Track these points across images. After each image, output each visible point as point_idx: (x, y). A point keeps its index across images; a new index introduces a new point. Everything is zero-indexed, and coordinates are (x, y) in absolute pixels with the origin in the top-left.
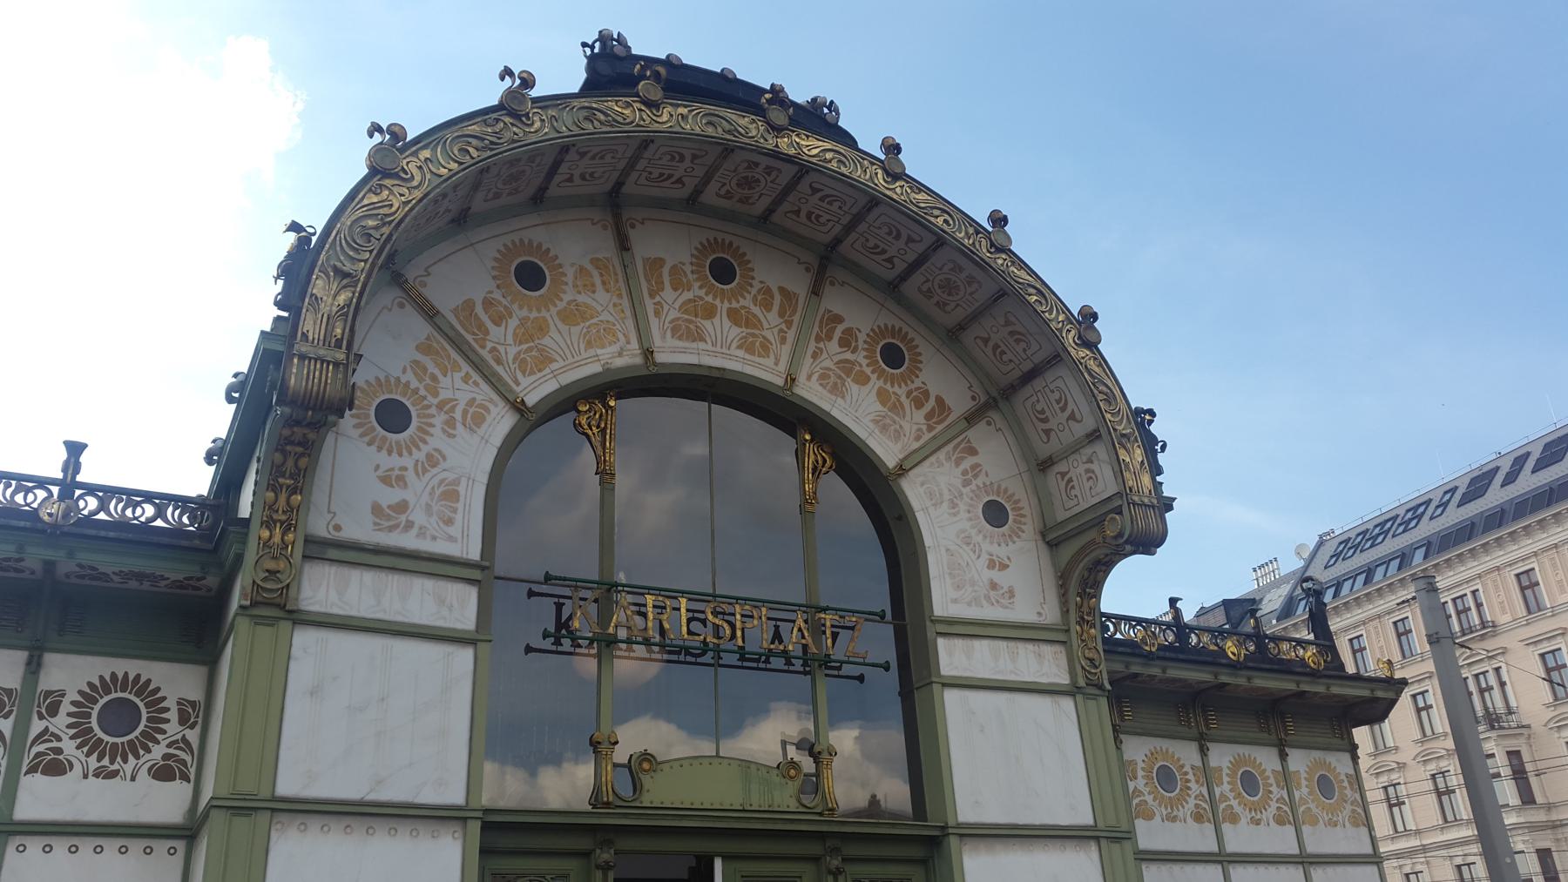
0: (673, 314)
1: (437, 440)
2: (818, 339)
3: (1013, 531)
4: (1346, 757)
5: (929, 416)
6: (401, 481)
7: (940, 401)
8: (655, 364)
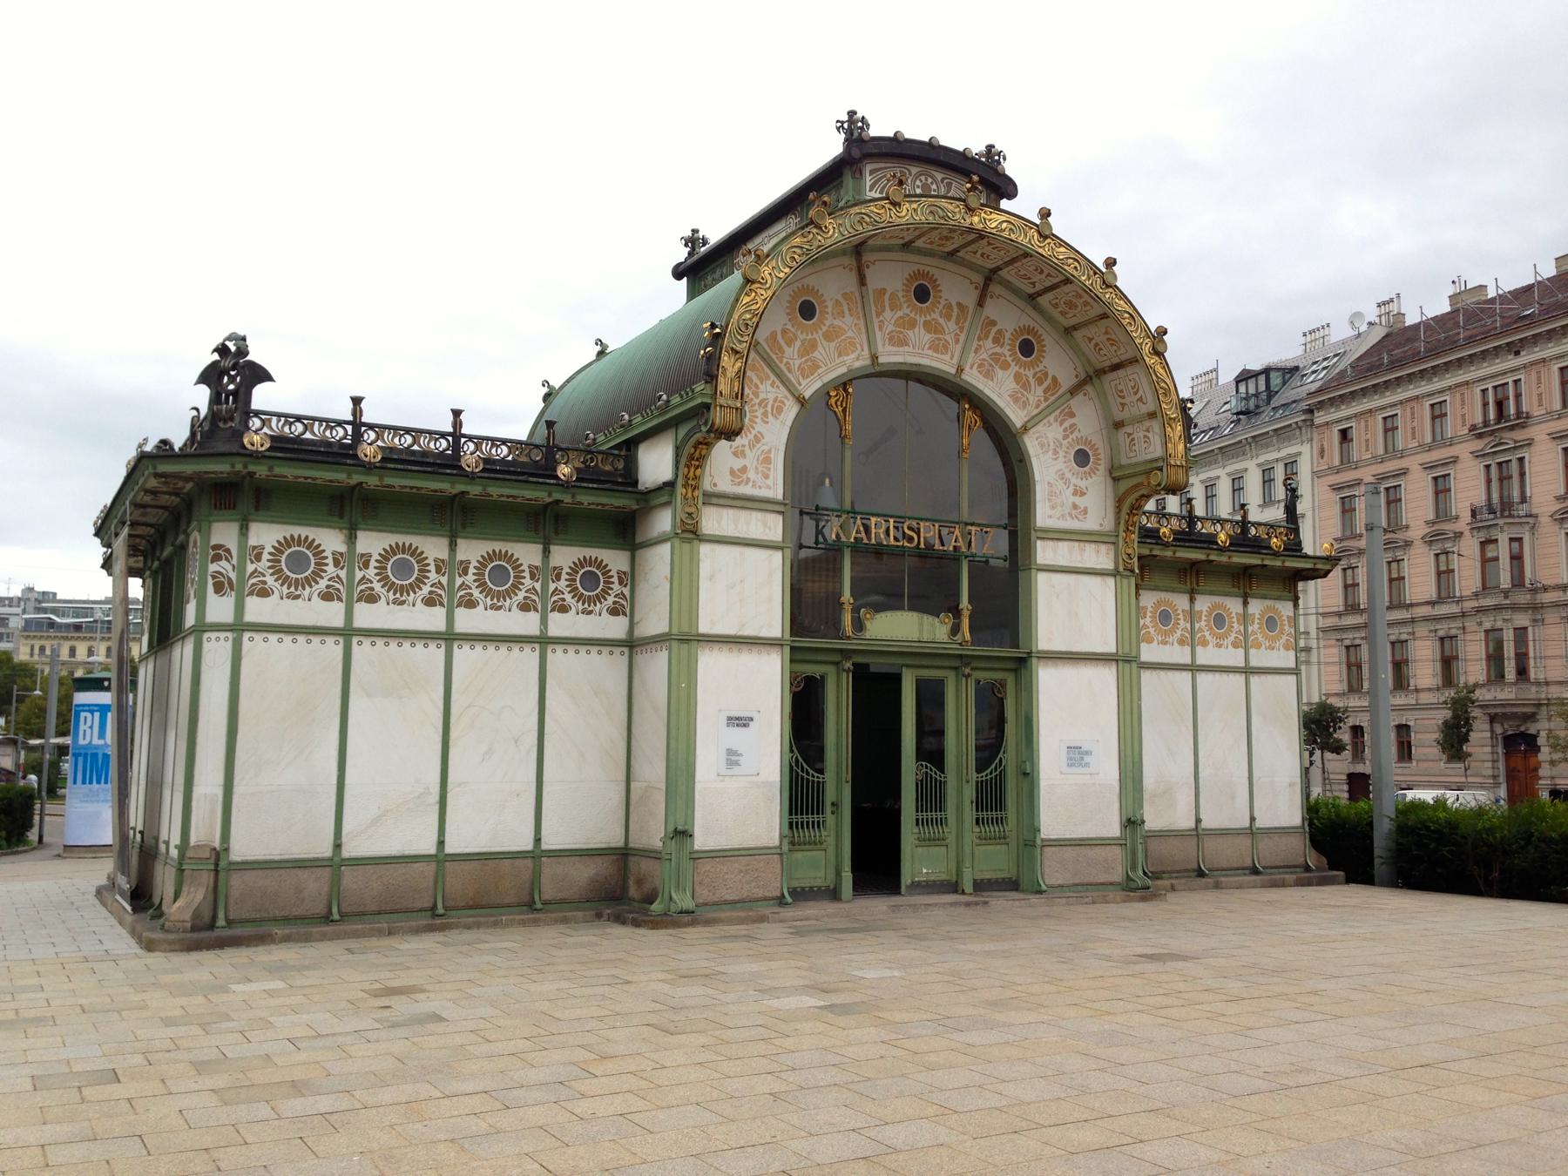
0: (891, 328)
2: (979, 339)
4: (1290, 604)
5: (1045, 391)
6: (743, 454)
7: (1055, 379)
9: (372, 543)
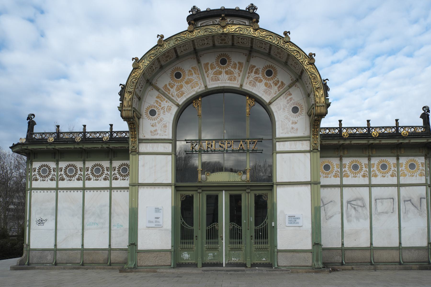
1: (162, 116)
3: (300, 114)
5: (279, 87)
7: (282, 83)
8: (208, 89)
9: (63, 165)
